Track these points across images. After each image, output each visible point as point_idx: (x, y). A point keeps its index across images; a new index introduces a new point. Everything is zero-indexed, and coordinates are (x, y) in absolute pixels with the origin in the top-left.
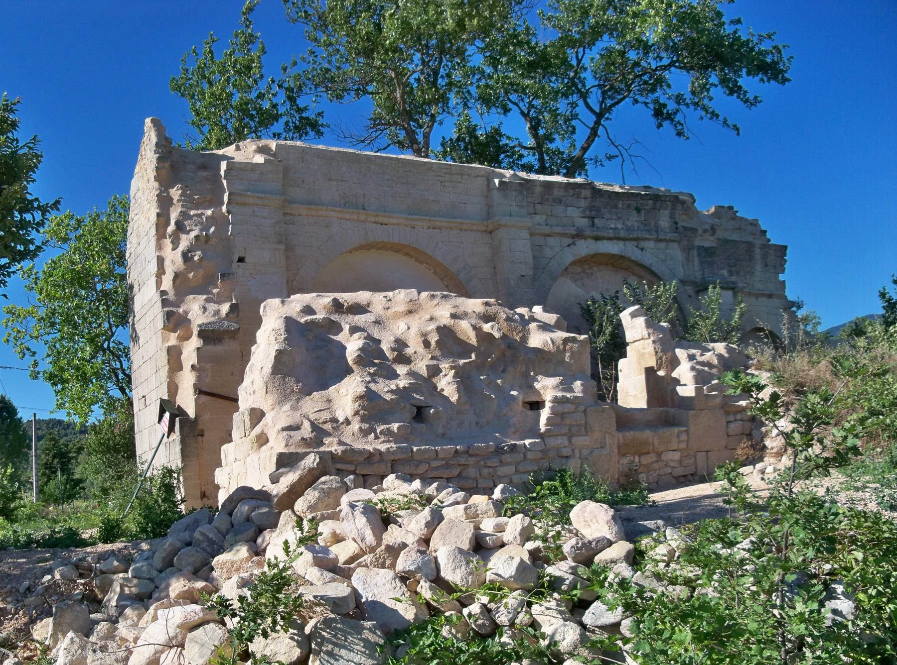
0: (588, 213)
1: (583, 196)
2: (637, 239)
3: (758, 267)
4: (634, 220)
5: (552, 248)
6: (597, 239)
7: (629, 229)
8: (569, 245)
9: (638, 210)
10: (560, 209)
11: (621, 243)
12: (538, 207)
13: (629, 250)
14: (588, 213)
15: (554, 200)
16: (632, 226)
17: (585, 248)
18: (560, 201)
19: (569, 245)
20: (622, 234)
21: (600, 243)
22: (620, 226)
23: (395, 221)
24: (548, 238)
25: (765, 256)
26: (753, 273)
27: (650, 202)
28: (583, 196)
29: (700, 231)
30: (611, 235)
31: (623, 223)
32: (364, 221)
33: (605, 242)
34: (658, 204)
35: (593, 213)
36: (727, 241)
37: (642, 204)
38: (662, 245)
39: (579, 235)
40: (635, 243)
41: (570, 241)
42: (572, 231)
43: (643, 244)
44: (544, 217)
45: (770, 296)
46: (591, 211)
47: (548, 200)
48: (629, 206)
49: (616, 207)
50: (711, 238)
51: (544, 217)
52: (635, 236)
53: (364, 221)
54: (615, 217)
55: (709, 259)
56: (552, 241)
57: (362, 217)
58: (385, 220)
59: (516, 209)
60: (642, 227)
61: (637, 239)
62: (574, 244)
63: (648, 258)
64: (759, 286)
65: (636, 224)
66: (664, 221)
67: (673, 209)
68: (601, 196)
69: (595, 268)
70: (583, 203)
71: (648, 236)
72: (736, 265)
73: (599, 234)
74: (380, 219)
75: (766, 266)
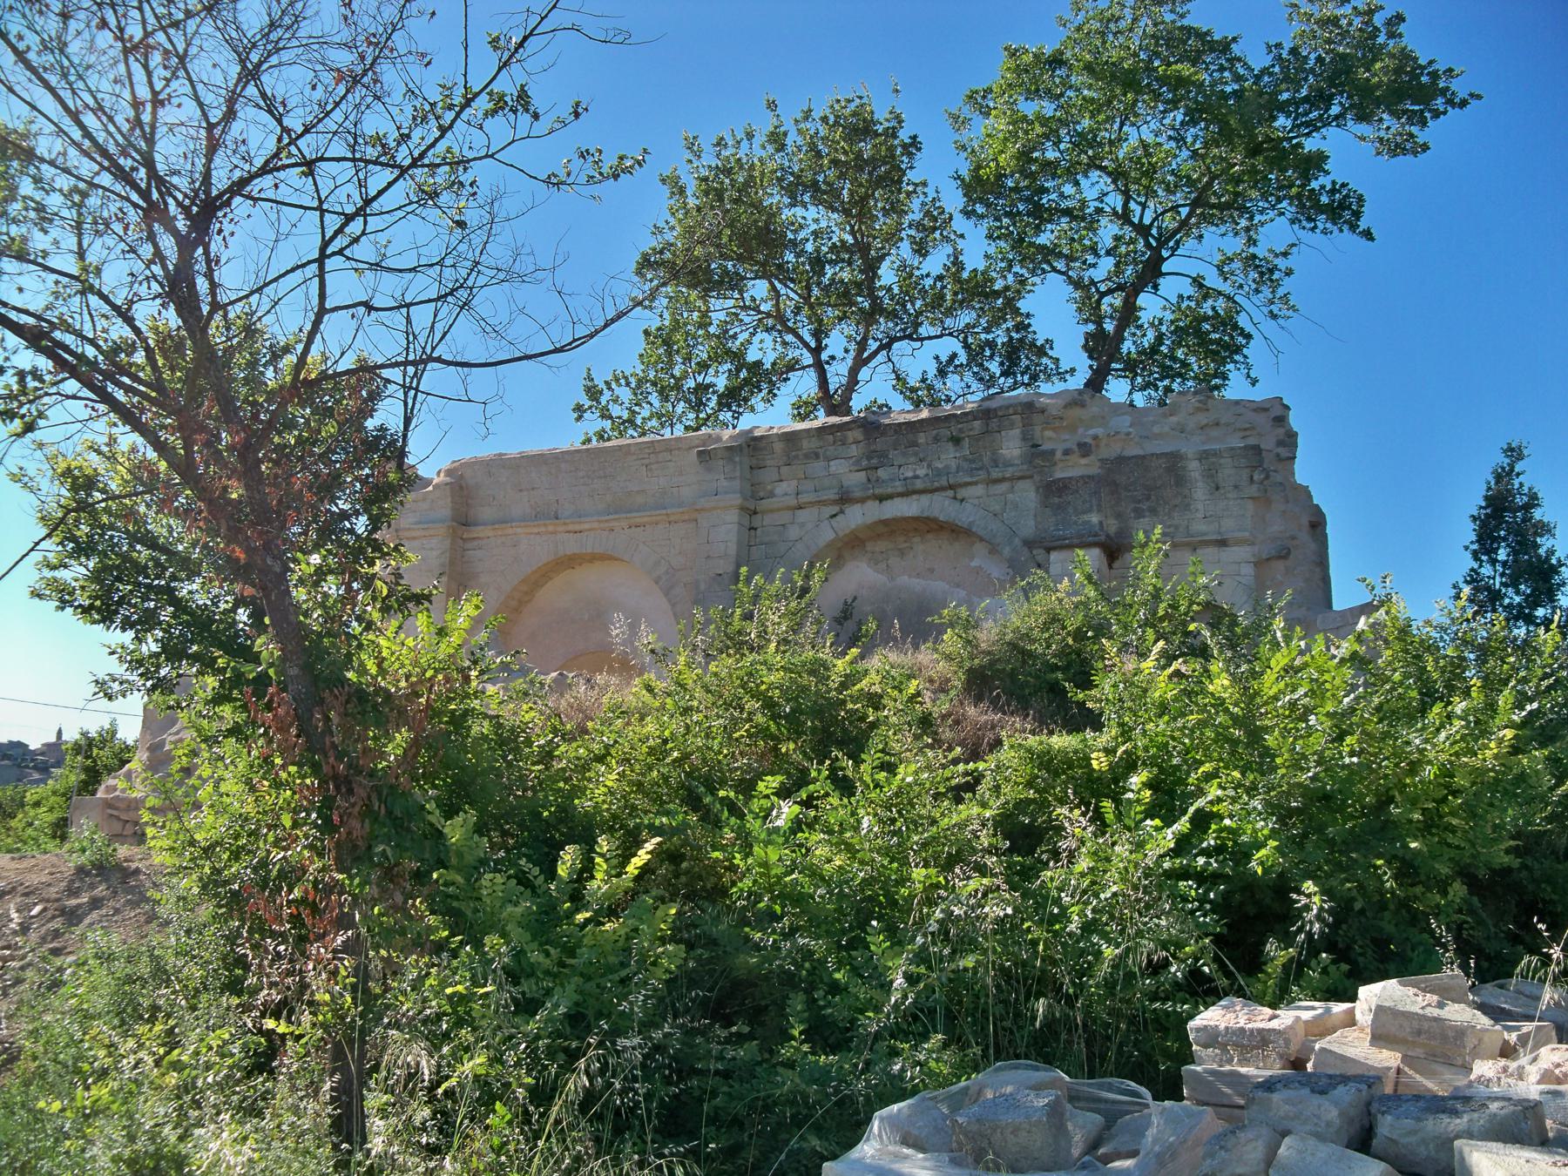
0: (865, 463)
1: (851, 440)
2: (951, 487)
3: (1200, 492)
4: (949, 457)
5: (802, 525)
6: (882, 499)
7: (939, 473)
8: (834, 516)
9: (956, 441)
10: (817, 467)
11: (925, 499)
12: (784, 470)
13: (940, 506)
14: (865, 463)
15: (807, 456)
16: (947, 467)
17: (857, 517)
18: (817, 456)
19: (834, 516)
20: (919, 485)
21: (888, 503)
22: (921, 472)
23: (586, 526)
24: (799, 512)
25: (1210, 473)
26: (1188, 505)
27: (977, 424)
28: (851, 440)
29: (1059, 455)
30: (900, 490)
31: (929, 466)
32: (555, 533)
33: (897, 501)
34: (994, 423)
35: (875, 461)
36: (1121, 460)
37: (961, 430)
38: (1004, 487)
39: (845, 499)
40: (950, 493)
41: (836, 509)
42: (831, 495)
43: (962, 493)
44: (795, 483)
45: (1222, 543)
46: (869, 458)
47: (796, 457)
48: (937, 439)
49: (915, 444)
50: (1083, 461)
51: (795, 483)
52: (944, 483)
53: (555, 533)
54: (912, 459)
55: (1056, 500)
56: (802, 515)
57: (551, 528)
58: (577, 527)
59: (725, 483)
60: (965, 465)
61: (951, 487)
62: (842, 512)
63: (965, 515)
64: (1199, 527)
65: (953, 464)
66: (1011, 447)
67: (1027, 424)
68: (883, 434)
69: (917, 539)
70: (854, 451)
71: (968, 479)
72: (1148, 498)
73: (877, 491)
74: (571, 527)
75: (1217, 488)
